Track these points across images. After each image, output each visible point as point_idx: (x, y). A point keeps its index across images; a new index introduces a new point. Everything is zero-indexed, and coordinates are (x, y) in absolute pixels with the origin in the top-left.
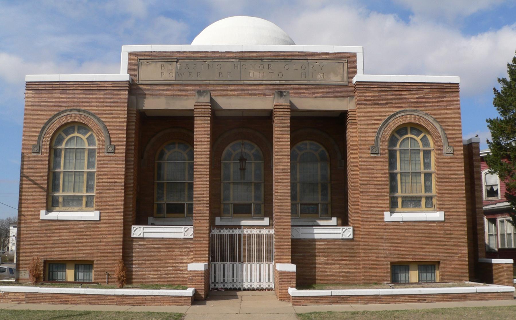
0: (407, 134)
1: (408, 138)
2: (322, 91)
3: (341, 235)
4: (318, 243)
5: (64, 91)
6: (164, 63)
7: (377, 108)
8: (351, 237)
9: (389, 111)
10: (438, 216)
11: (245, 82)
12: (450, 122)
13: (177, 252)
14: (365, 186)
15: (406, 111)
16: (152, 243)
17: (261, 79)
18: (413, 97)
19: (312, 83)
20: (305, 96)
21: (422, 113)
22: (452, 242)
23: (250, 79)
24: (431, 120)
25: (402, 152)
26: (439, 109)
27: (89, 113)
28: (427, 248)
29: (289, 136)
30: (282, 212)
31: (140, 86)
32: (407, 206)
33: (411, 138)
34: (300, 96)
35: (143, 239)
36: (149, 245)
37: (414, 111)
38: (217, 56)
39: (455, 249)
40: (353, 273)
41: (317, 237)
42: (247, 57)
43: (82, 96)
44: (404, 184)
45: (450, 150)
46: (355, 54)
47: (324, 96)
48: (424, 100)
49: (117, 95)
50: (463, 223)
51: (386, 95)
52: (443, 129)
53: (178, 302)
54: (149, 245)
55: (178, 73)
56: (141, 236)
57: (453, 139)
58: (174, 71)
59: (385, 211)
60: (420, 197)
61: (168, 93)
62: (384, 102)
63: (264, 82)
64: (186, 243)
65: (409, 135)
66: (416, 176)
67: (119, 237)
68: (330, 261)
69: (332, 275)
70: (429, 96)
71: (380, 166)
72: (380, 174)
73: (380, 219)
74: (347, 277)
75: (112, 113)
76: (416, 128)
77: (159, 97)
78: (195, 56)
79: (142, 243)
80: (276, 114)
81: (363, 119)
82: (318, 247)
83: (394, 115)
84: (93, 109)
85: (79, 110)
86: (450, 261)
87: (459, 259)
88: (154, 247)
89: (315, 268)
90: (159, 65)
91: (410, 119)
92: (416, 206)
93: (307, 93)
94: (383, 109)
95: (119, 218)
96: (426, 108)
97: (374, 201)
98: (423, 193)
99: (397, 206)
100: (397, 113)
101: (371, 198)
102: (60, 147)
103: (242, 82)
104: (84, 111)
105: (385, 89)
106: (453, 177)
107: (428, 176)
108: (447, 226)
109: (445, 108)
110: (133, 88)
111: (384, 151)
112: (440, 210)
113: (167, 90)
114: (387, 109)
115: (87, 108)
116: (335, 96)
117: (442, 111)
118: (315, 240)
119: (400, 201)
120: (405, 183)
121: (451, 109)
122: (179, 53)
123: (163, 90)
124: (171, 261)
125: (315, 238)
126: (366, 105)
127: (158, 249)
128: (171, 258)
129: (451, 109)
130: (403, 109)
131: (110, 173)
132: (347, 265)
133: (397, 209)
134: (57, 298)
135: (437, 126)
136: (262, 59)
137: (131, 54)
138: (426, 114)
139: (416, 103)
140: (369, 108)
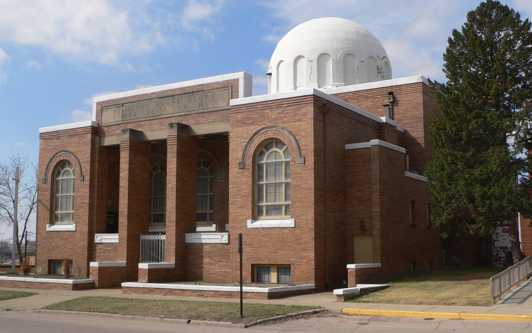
0: (272, 148)
1: (273, 152)
2: (213, 117)
3: (220, 240)
4: (205, 247)
5: (58, 138)
6: (115, 109)
7: (245, 128)
8: (227, 242)
10: (288, 222)
11: (163, 116)
12: (303, 134)
14: (235, 198)
15: (267, 128)
16: (106, 246)
17: (173, 112)
18: (272, 114)
19: (207, 110)
20: (201, 123)
22: (301, 246)
23: (167, 113)
24: (287, 133)
25: (267, 164)
26: (294, 122)
27: (71, 153)
28: (280, 252)
29: (175, 160)
31: (103, 128)
32: (271, 214)
33: (276, 151)
34: (198, 124)
35: (101, 243)
36: (105, 248)
37: (273, 127)
38: (146, 97)
39: (304, 254)
40: (229, 273)
41: (204, 241)
42: (164, 95)
43: (67, 140)
44: (269, 194)
45: (302, 160)
47: (214, 121)
48: (282, 115)
49: (86, 138)
50: (311, 229)
51: (252, 115)
53: (66, 288)
54: (105, 248)
55: (124, 116)
56: (100, 242)
57: (305, 149)
59: (248, 219)
60: (281, 205)
62: (250, 122)
63: (175, 115)
65: (274, 149)
66: (279, 186)
67: (86, 243)
68: (213, 262)
69: (214, 274)
70: (287, 110)
71: (245, 179)
72: (245, 186)
73: (244, 226)
74: (224, 276)
75: (83, 151)
76: (278, 143)
77: (112, 135)
78: (133, 100)
79: (101, 246)
80: (169, 143)
81: (234, 139)
82: (205, 250)
83: (258, 132)
84: (73, 149)
85: (65, 151)
86: (299, 265)
87: (306, 263)
88: (107, 250)
89: (202, 268)
90: (113, 110)
91: (270, 134)
92: (278, 214)
93: (202, 120)
94: (250, 128)
95: (86, 229)
97: (240, 210)
98: (283, 202)
99: (262, 214)
100: (260, 130)
101: (238, 208)
102: (58, 179)
103: (161, 117)
104: (68, 151)
105: (253, 109)
106: (304, 186)
108: (297, 231)
109: (300, 120)
110: (96, 131)
111: (249, 165)
112: (292, 217)
118: (203, 244)
119: (264, 209)
120: (270, 193)
121: (305, 121)
122: (124, 98)
123: (115, 130)
125: (203, 242)
126: (237, 126)
127: (109, 251)
129: (305, 121)
130: (265, 126)
131: (81, 196)
132: (224, 266)
133: (262, 217)
135: (292, 138)
136: (174, 96)
137: (98, 104)
138: (283, 128)
139: (276, 119)
140: (240, 129)
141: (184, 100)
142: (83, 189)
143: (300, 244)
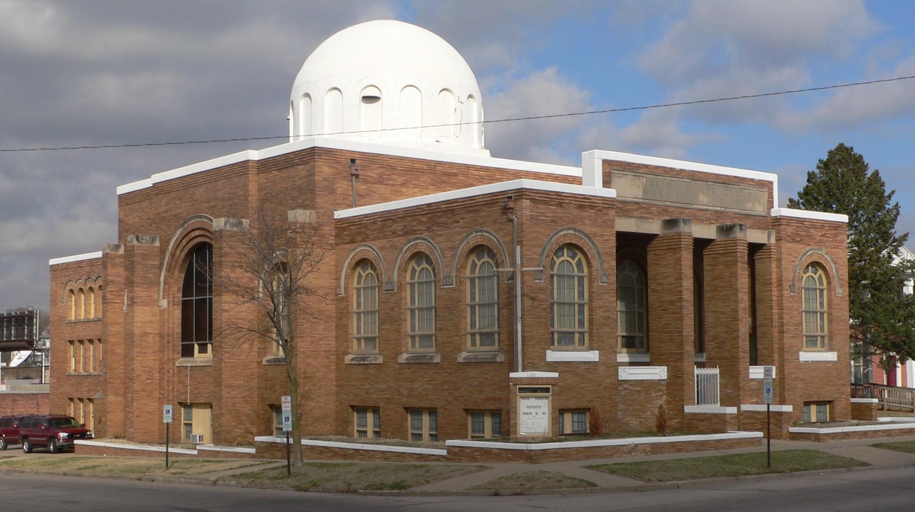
5: (560, 205)
9: (808, 248)
10: (832, 356)
13: (654, 395)
18: (817, 234)
19: (743, 212)
21: (823, 252)
27: (584, 234)
30: (744, 352)
43: (576, 212)
46: (771, 183)
48: (825, 239)
49: (606, 214)
52: (837, 269)
55: (645, 192)
58: (641, 188)
61: (637, 213)
62: (798, 239)
63: (709, 208)
64: (660, 385)
75: (603, 236)
77: (631, 217)
84: (588, 229)
96: (826, 247)
104: (580, 231)
107: (822, 313)
109: (837, 247)
113: (637, 209)
114: (801, 246)
115: (581, 228)
116: (759, 228)
117: (836, 250)
124: (649, 405)
127: (639, 392)
128: (649, 402)
131: (604, 307)
134: (674, 447)
135: (833, 265)
139: (820, 242)
141: (720, 188)
142: (606, 296)
143: (840, 379)
